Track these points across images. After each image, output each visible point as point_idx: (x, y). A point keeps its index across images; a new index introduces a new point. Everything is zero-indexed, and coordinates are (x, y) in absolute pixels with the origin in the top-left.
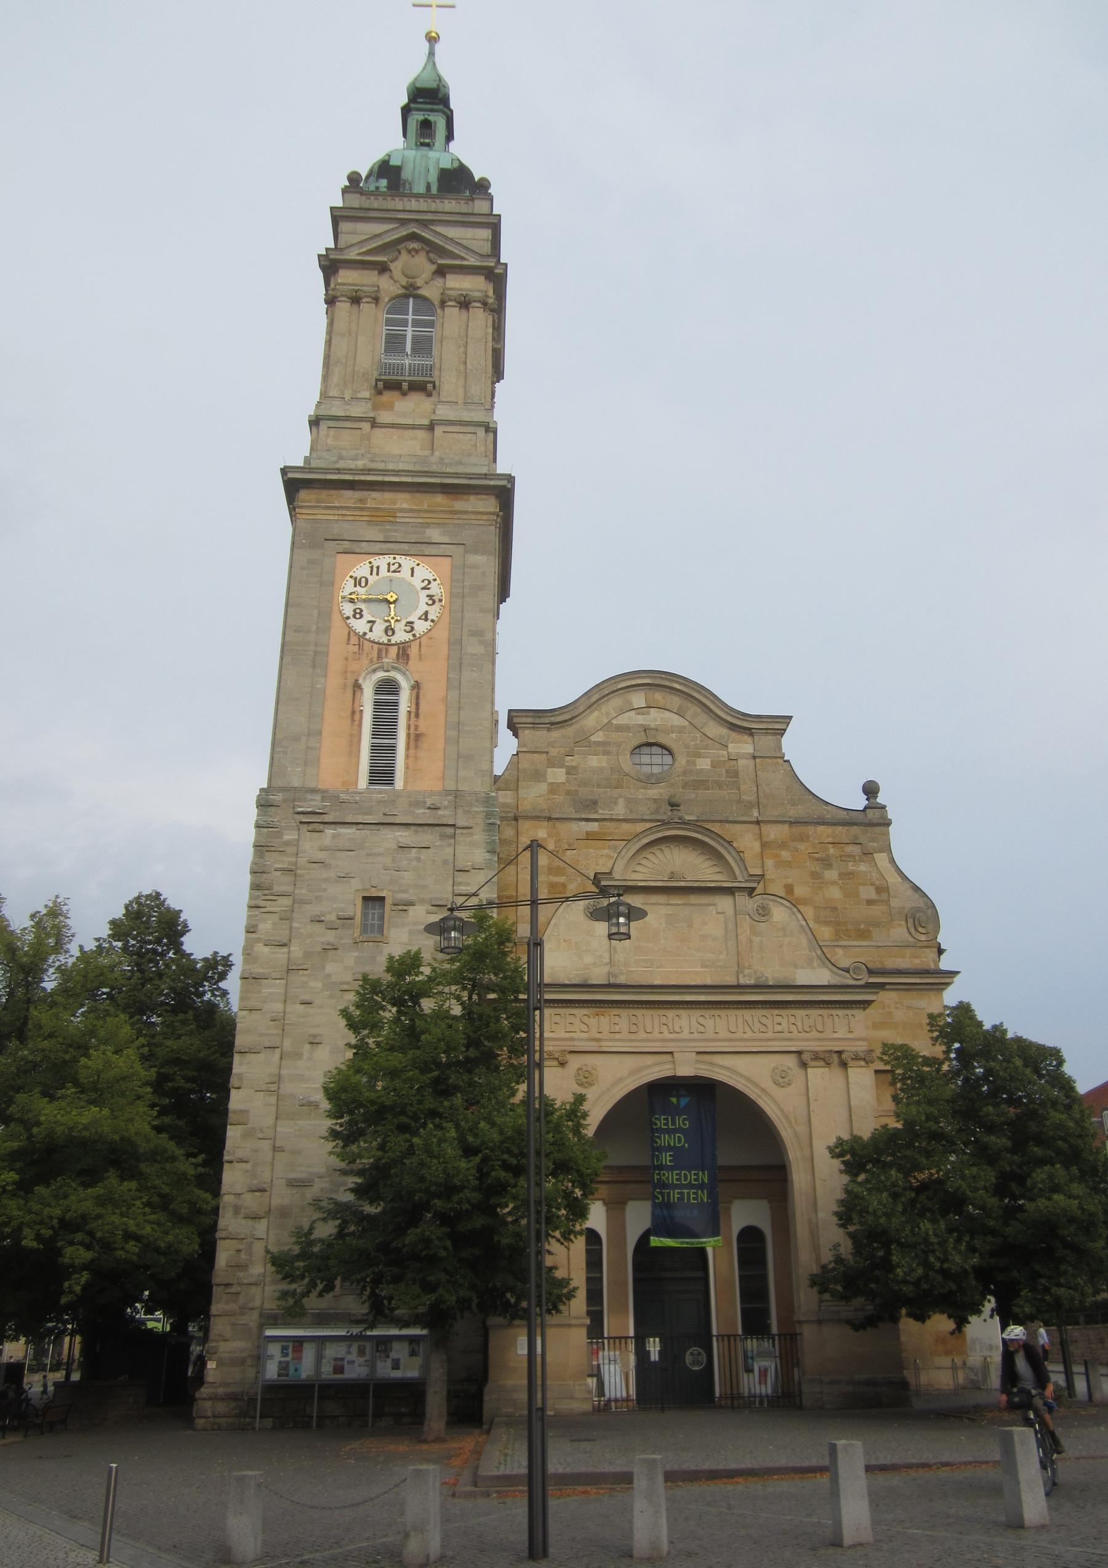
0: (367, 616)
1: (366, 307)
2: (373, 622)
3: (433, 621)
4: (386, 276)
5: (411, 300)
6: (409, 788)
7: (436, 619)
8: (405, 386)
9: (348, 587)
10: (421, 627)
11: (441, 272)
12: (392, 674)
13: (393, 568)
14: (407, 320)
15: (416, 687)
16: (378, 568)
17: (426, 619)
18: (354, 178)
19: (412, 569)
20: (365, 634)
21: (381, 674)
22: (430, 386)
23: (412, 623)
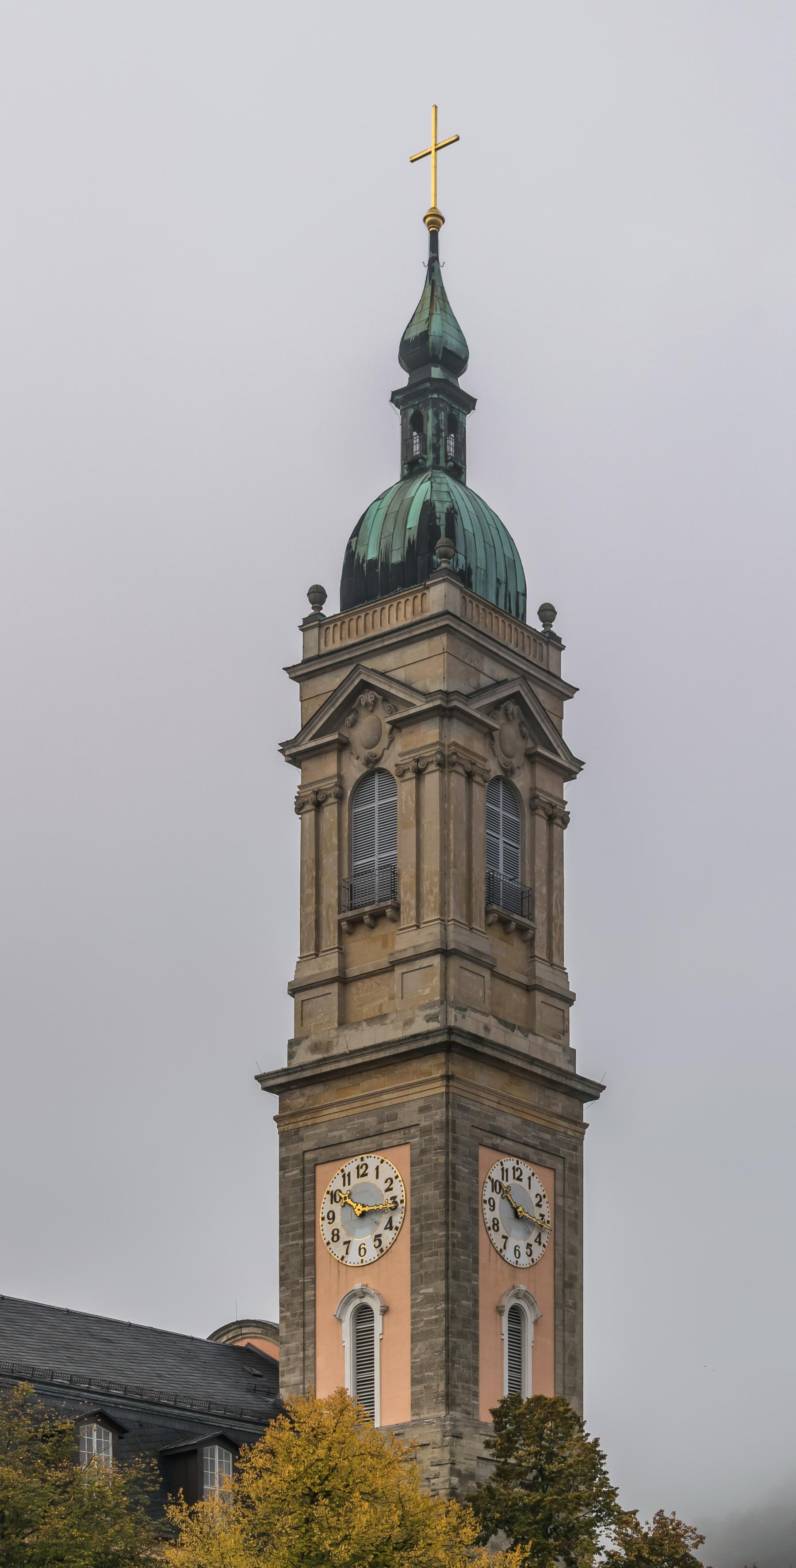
0: (344, 1238)
1: (330, 813)
2: (348, 1243)
3: (397, 1228)
4: (345, 756)
5: (376, 777)
6: (383, 1425)
7: (399, 1226)
8: (367, 919)
9: (325, 1206)
10: (388, 1237)
11: (397, 726)
12: (367, 1300)
13: (361, 1171)
14: (373, 809)
15: (385, 1311)
16: (349, 1175)
17: (391, 1228)
18: (317, 595)
19: (377, 1168)
20: (343, 1258)
21: (357, 1302)
22: (389, 912)
23: (380, 1235)
